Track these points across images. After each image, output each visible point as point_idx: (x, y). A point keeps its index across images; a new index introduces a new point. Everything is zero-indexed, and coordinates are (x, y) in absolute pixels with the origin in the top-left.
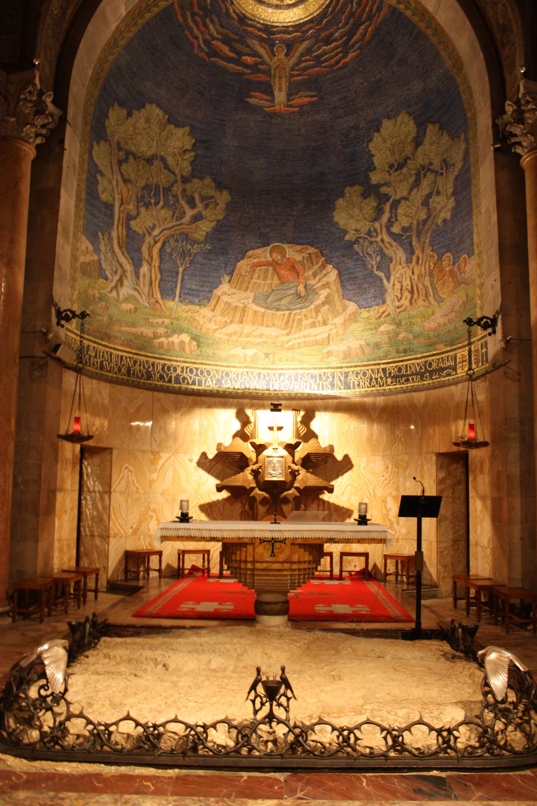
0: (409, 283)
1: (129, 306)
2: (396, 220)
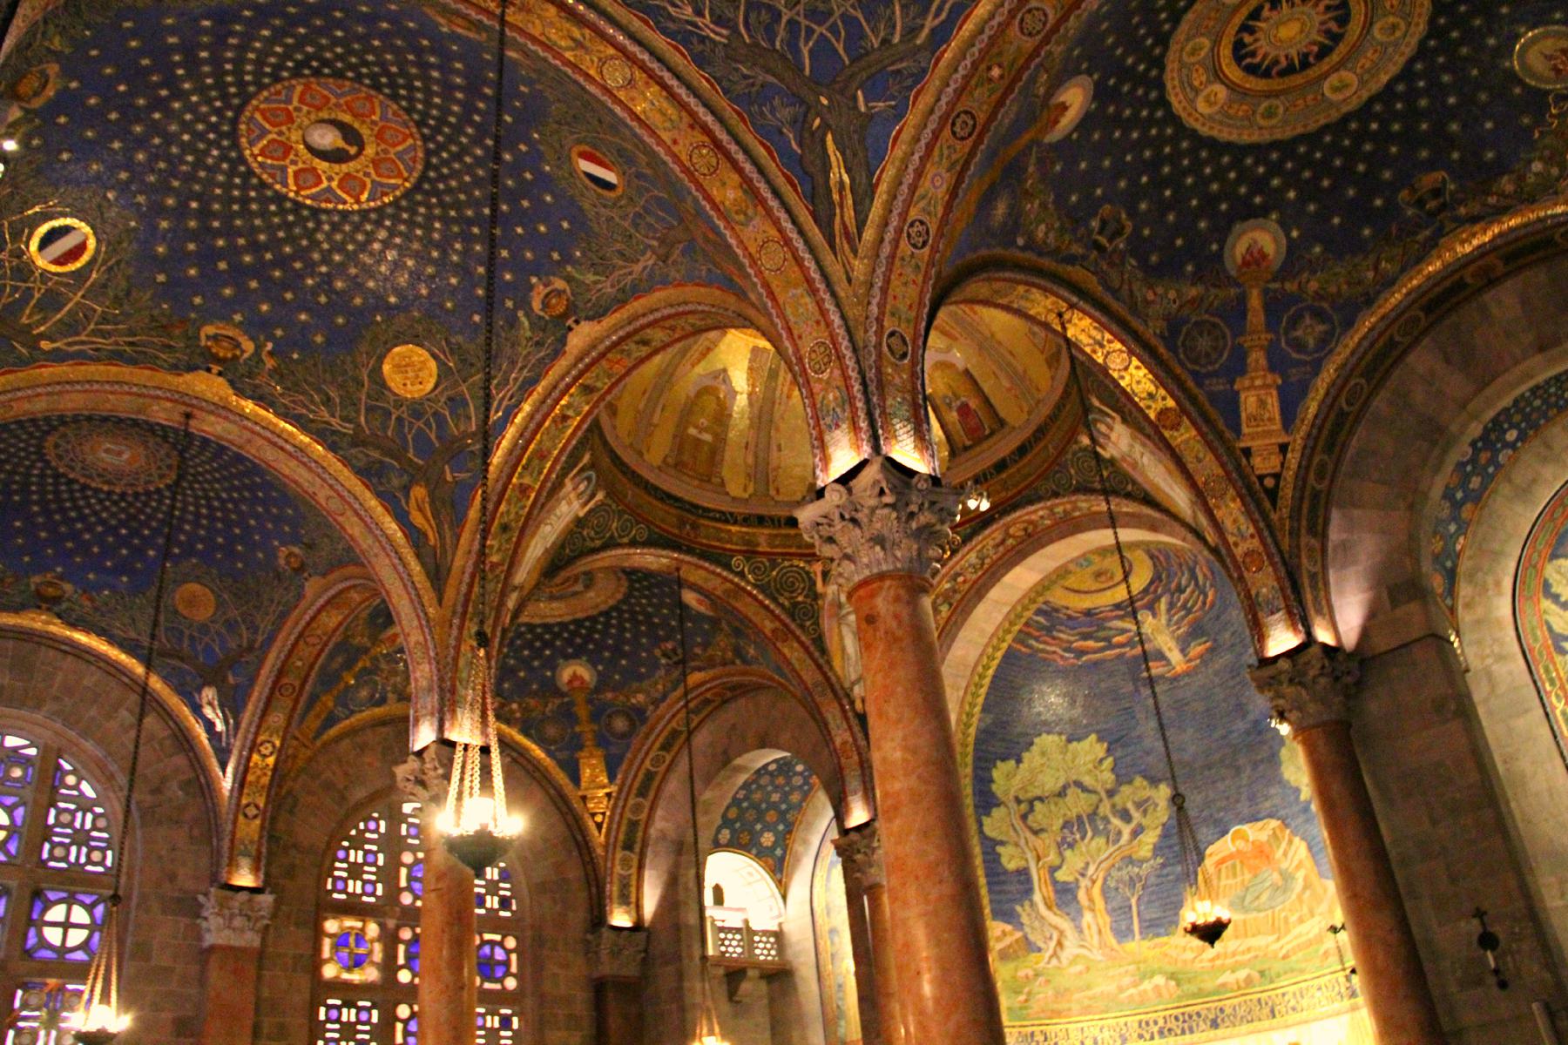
1: (1079, 968)
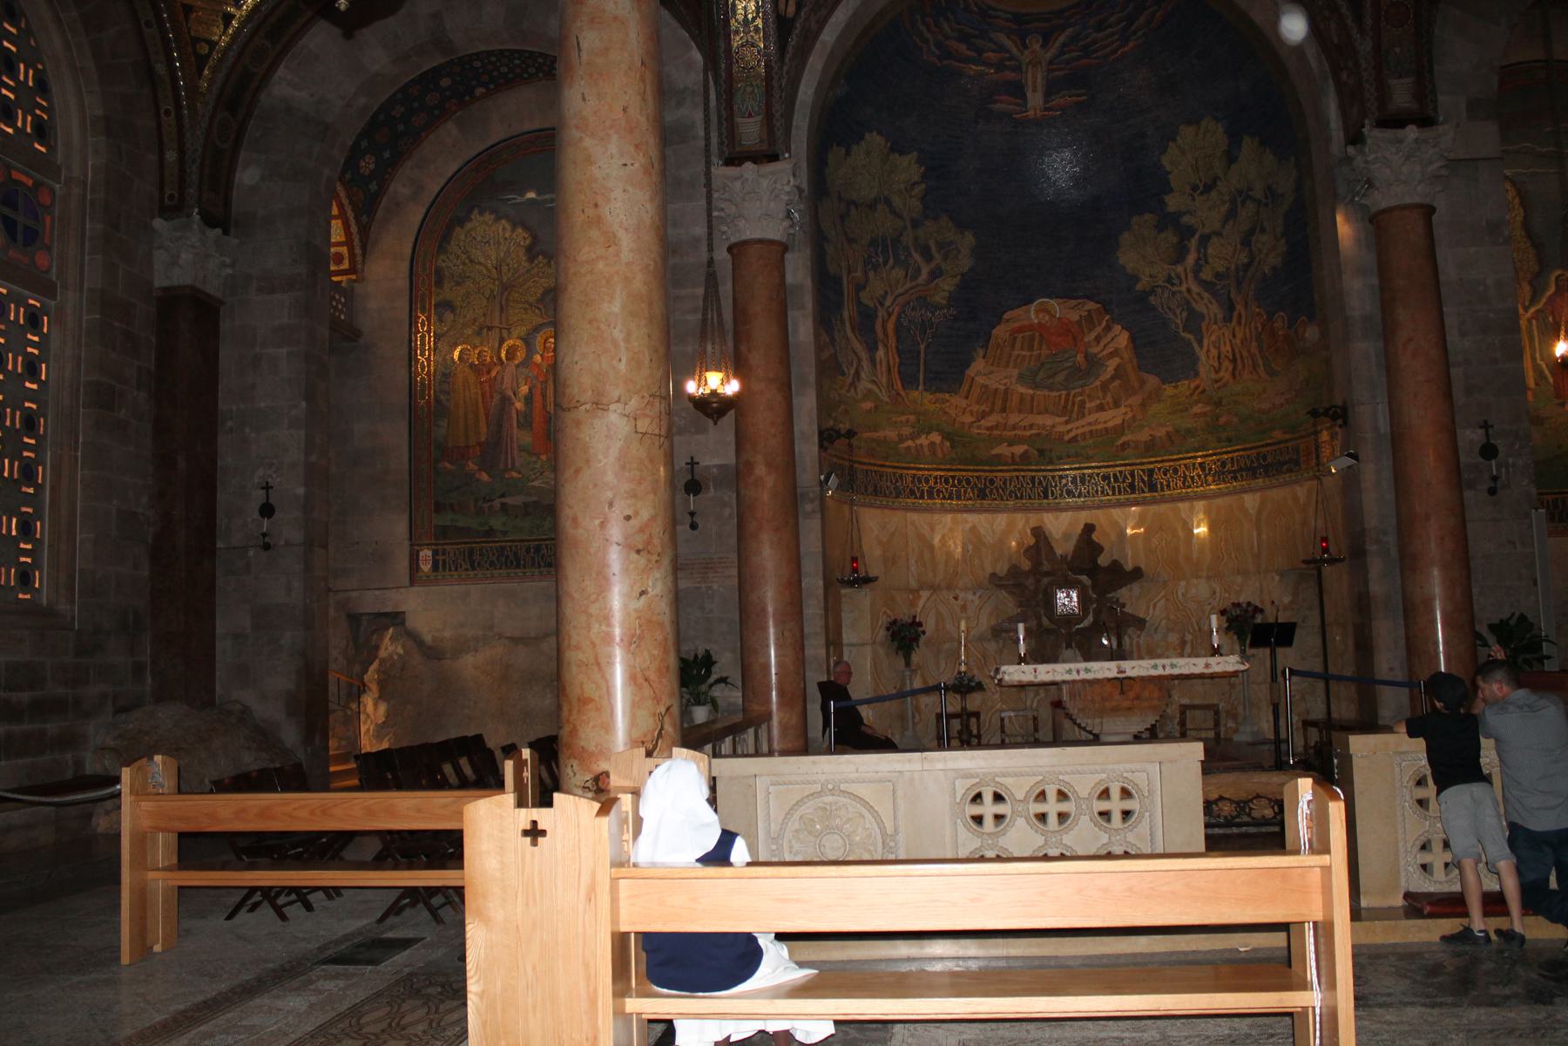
0: (1229, 349)
1: (868, 405)
2: (1207, 262)
